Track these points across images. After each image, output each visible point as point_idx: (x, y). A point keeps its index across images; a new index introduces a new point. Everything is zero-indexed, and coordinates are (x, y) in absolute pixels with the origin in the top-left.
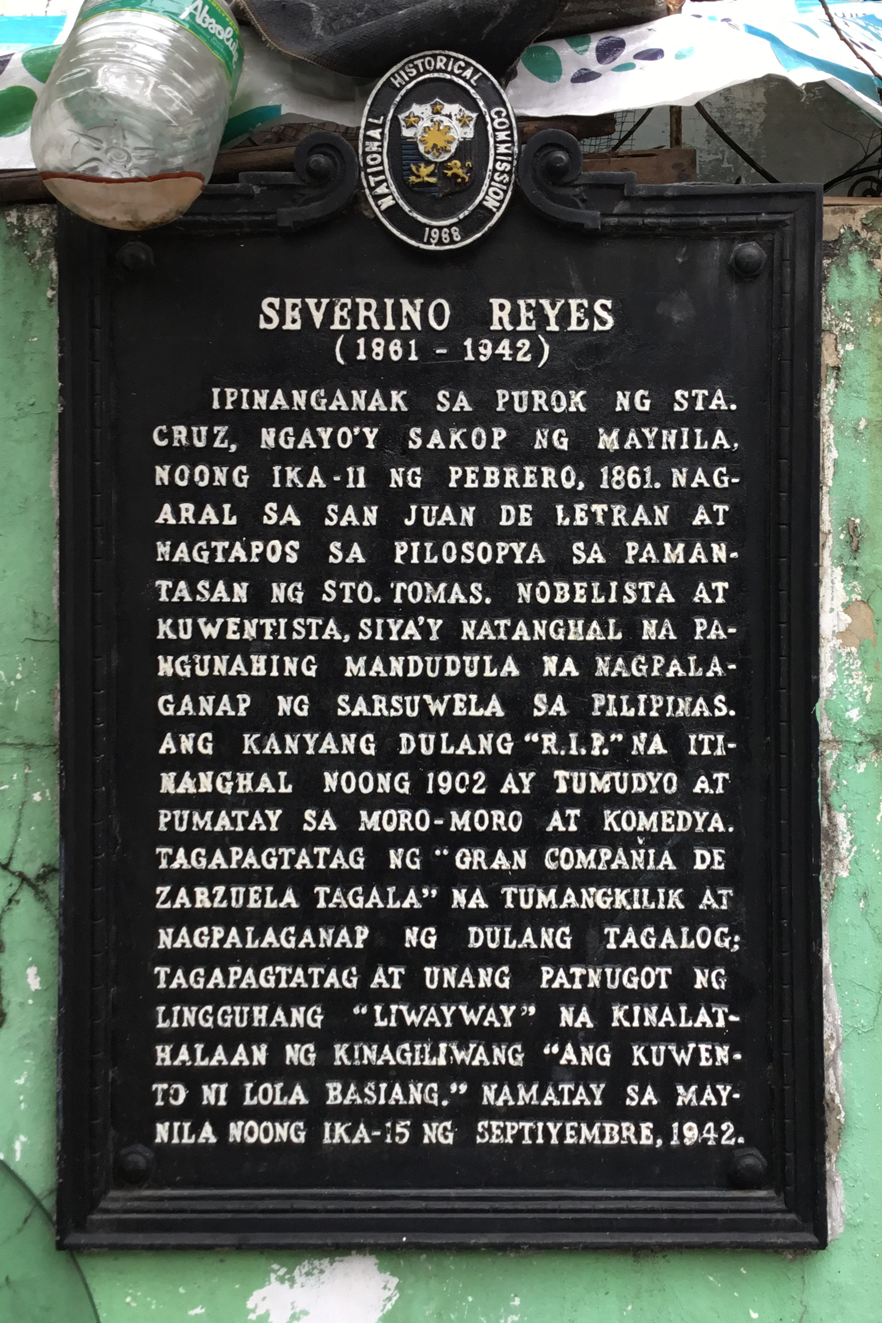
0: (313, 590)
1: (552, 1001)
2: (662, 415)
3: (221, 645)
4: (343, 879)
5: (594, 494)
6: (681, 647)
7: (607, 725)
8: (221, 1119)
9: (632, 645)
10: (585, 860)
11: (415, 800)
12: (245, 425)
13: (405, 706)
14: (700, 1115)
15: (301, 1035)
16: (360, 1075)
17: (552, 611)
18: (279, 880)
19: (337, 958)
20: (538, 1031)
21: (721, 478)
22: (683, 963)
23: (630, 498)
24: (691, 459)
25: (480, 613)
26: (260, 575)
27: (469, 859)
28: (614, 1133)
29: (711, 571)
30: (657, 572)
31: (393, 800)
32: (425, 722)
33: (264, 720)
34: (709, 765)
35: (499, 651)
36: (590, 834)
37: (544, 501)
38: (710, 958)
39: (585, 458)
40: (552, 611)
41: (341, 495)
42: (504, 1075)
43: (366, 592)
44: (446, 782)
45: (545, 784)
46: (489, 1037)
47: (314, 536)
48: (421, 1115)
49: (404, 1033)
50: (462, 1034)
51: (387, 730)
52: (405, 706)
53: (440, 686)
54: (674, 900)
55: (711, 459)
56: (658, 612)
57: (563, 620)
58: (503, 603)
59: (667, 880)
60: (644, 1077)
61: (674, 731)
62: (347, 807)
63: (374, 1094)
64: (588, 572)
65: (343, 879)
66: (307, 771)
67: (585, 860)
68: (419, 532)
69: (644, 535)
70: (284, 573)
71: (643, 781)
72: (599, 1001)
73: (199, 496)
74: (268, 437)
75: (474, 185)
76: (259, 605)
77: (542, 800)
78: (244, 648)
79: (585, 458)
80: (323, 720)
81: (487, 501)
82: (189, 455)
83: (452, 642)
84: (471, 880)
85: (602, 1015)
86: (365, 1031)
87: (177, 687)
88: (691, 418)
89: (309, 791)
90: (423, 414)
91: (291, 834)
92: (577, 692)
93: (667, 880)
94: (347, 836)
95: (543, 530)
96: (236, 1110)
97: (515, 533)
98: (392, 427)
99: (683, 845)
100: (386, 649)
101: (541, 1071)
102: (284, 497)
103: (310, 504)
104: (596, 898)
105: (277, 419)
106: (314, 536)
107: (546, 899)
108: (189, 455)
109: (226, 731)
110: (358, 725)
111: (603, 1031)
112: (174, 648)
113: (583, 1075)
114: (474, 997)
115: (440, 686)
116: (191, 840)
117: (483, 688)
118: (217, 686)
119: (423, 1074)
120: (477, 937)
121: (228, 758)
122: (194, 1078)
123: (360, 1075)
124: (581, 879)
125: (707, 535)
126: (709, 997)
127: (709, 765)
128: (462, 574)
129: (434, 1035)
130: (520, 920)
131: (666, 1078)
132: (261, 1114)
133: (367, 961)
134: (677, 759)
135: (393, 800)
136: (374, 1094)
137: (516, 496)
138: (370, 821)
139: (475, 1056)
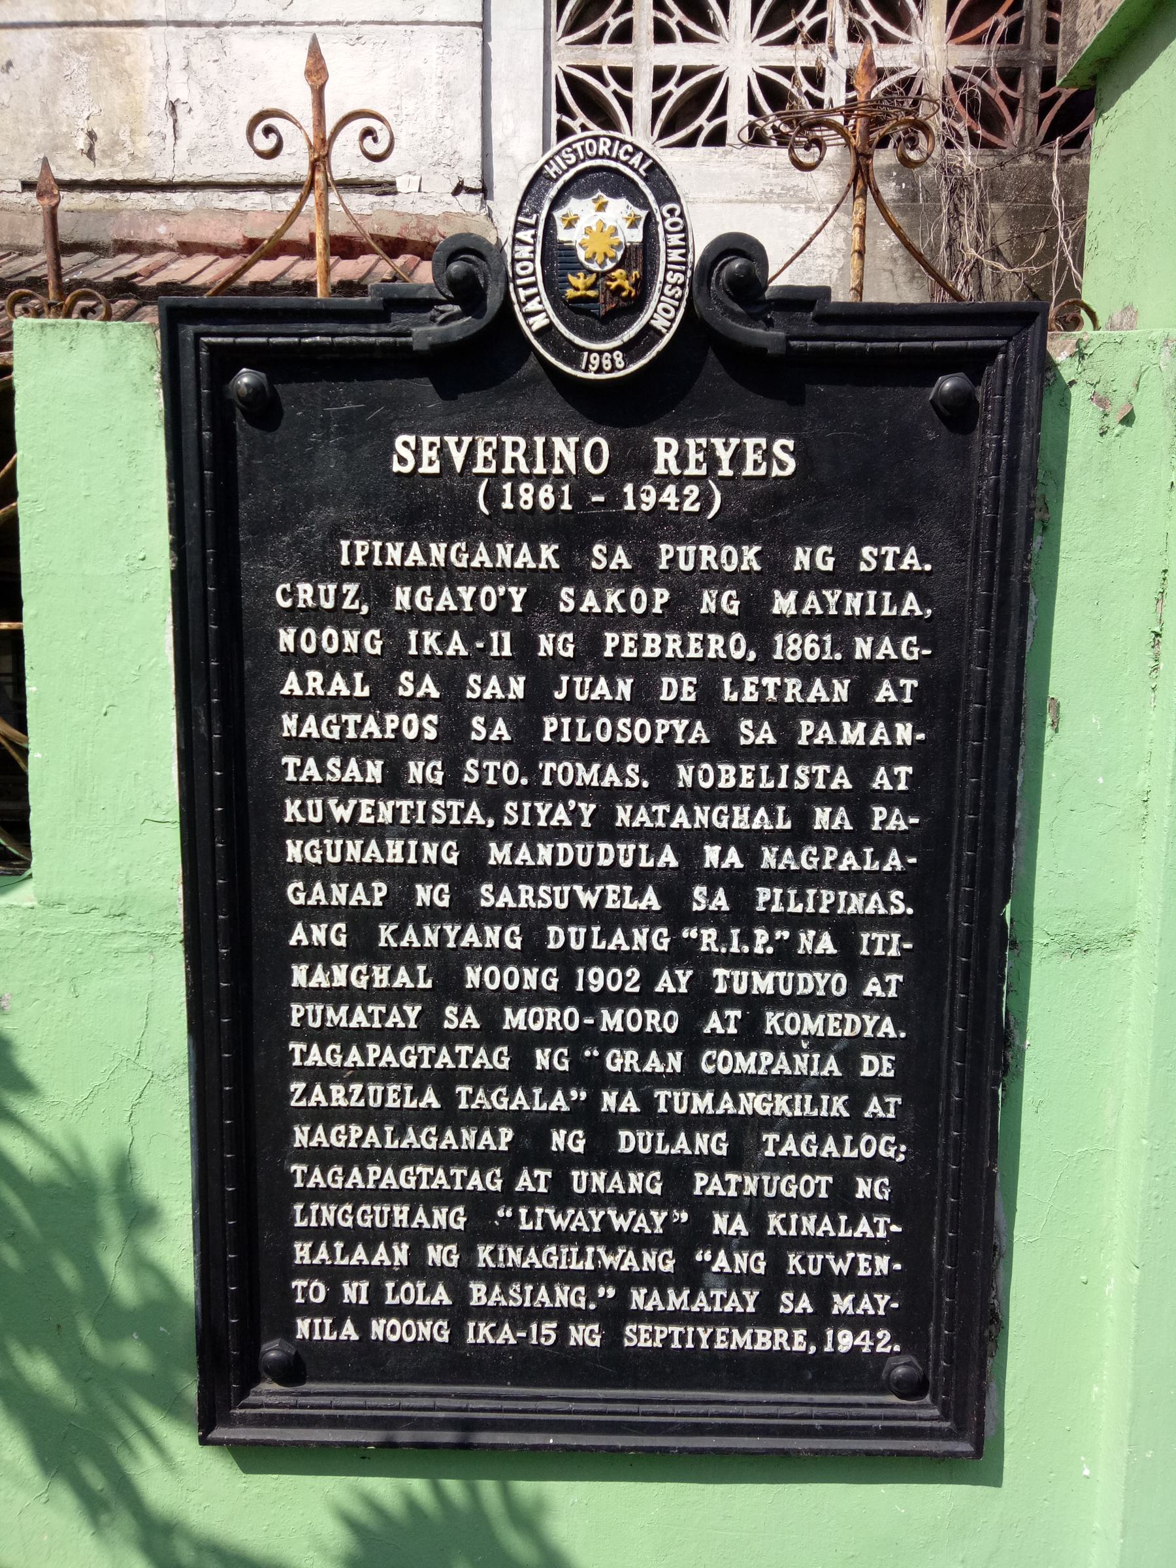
0: (454, 769)
1: (704, 1208)
2: (846, 576)
3: (352, 829)
4: (485, 1079)
5: (765, 665)
6: (858, 837)
7: (771, 921)
8: (362, 1317)
9: (801, 835)
10: (745, 1063)
11: (565, 996)
12: (378, 583)
13: (552, 896)
14: (855, 1323)
15: (443, 1236)
16: (505, 1277)
17: (713, 797)
18: (418, 1079)
19: (479, 1160)
20: (689, 1238)
21: (910, 649)
22: (845, 1173)
23: (806, 671)
24: (876, 626)
25: (636, 797)
26: (395, 753)
27: (621, 1060)
28: (767, 1339)
29: (892, 754)
30: (833, 754)
31: (539, 997)
32: (574, 914)
33: (400, 909)
34: (882, 966)
35: (655, 839)
36: (751, 1036)
37: (708, 672)
38: (873, 1167)
39: (758, 623)
40: (713, 797)
41: (481, 662)
42: (654, 1281)
43: (511, 773)
44: (597, 979)
45: (702, 984)
46: (639, 1242)
47: (454, 710)
48: (566, 1317)
49: (549, 1236)
50: (610, 1238)
51: (534, 923)
52: (552, 896)
53: (592, 876)
54: (838, 1106)
55: (899, 627)
56: (832, 798)
57: (727, 803)
58: (661, 787)
59: (831, 1085)
60: (800, 1284)
61: (846, 929)
62: (490, 1005)
63: (518, 1296)
64: (757, 753)
65: (485, 1079)
66: (447, 967)
67: (745, 1063)
68: (570, 707)
69: (820, 712)
70: (421, 748)
71: (810, 982)
72: (756, 1210)
73: (327, 664)
74: (402, 598)
75: (637, 303)
76: (394, 785)
77: (700, 1001)
78: (379, 832)
79: (758, 623)
80: (465, 910)
81: (647, 673)
82: (316, 617)
83: (605, 828)
84: (621, 1082)
85: (757, 1222)
86: (510, 1234)
87: (309, 873)
88: (877, 580)
89: (449, 986)
90: (575, 572)
91: (431, 1030)
92: (739, 886)
93: (831, 1085)
94: (490, 1034)
95: (707, 706)
96: (377, 1307)
97: (675, 709)
98: (542, 589)
99: (850, 1051)
100: (533, 835)
101: (691, 1276)
102: (421, 665)
103: (450, 674)
104: (754, 1103)
105: (413, 576)
106: (454, 710)
107: (702, 1103)
108: (316, 617)
109: (362, 922)
110: (502, 917)
111: (757, 1239)
112: (304, 831)
113: (736, 1282)
114: (623, 1203)
115: (592, 876)
116: (324, 1036)
117: (638, 878)
118: (351, 873)
119: (570, 1278)
120: (628, 1141)
121: (363, 949)
122: (334, 1276)
123: (505, 1277)
124: (738, 1084)
125: (891, 714)
126: (871, 1207)
127: (882, 966)
128: (616, 753)
129: (582, 1239)
130: (672, 1125)
131: (823, 1287)
132: (401, 1312)
133: (512, 1162)
134: (849, 960)
135: (539, 997)
136: (518, 1296)
137: (679, 667)
138: (514, 1019)
139: (623, 1260)
